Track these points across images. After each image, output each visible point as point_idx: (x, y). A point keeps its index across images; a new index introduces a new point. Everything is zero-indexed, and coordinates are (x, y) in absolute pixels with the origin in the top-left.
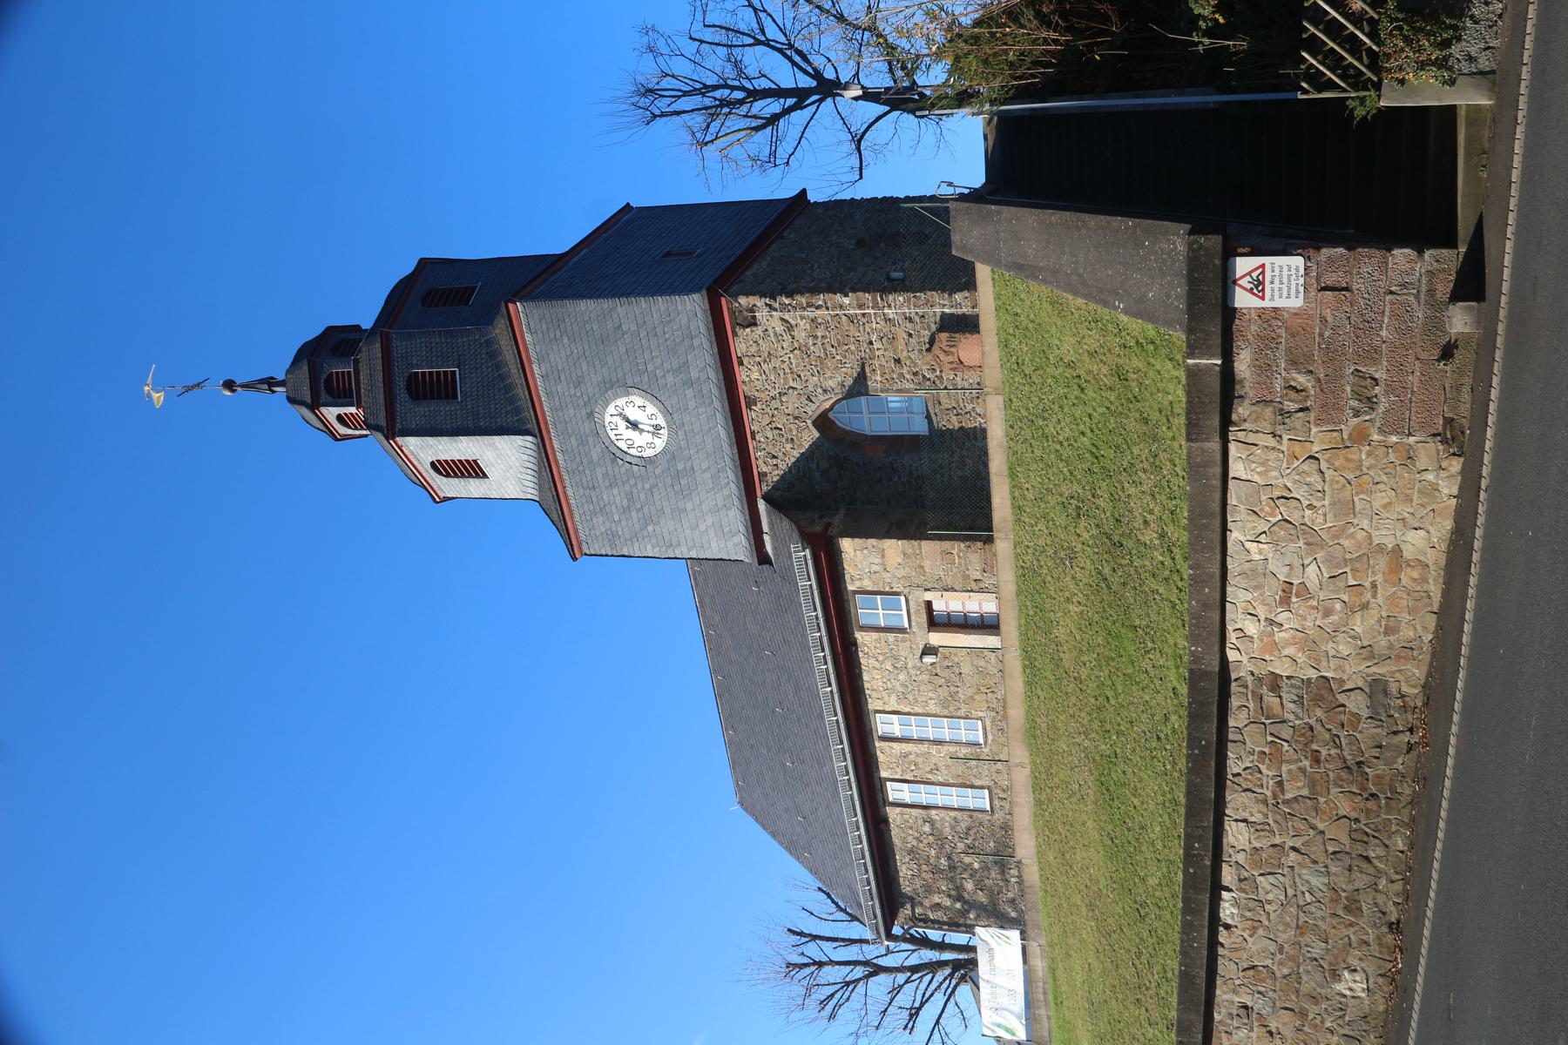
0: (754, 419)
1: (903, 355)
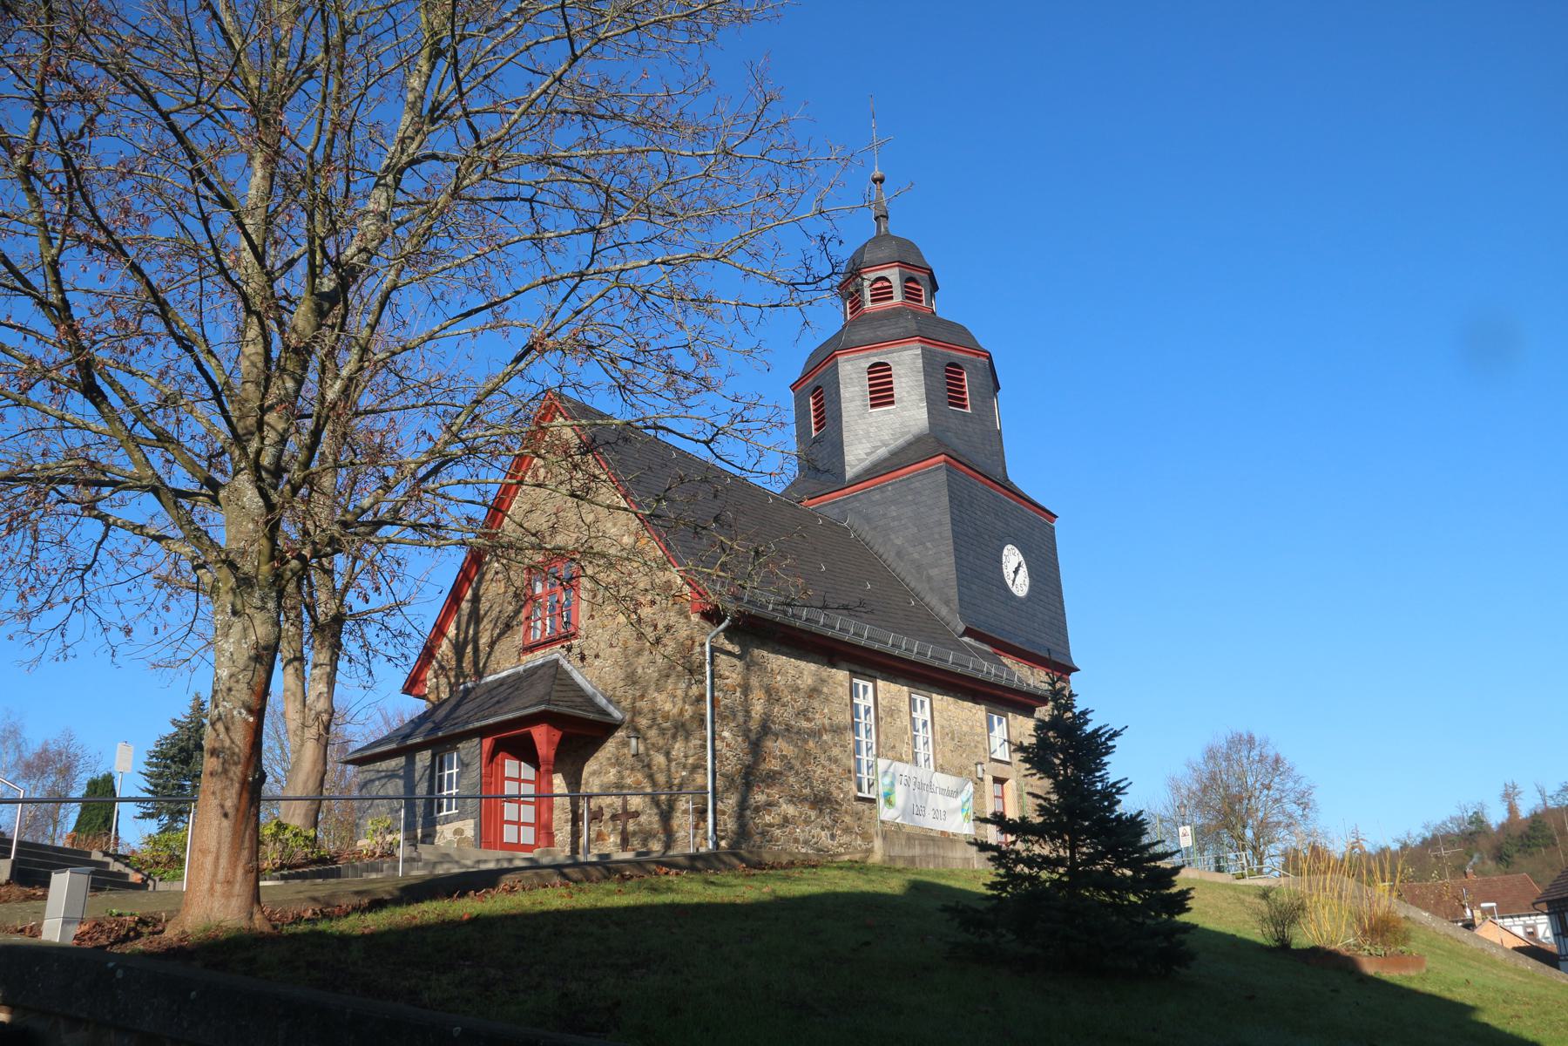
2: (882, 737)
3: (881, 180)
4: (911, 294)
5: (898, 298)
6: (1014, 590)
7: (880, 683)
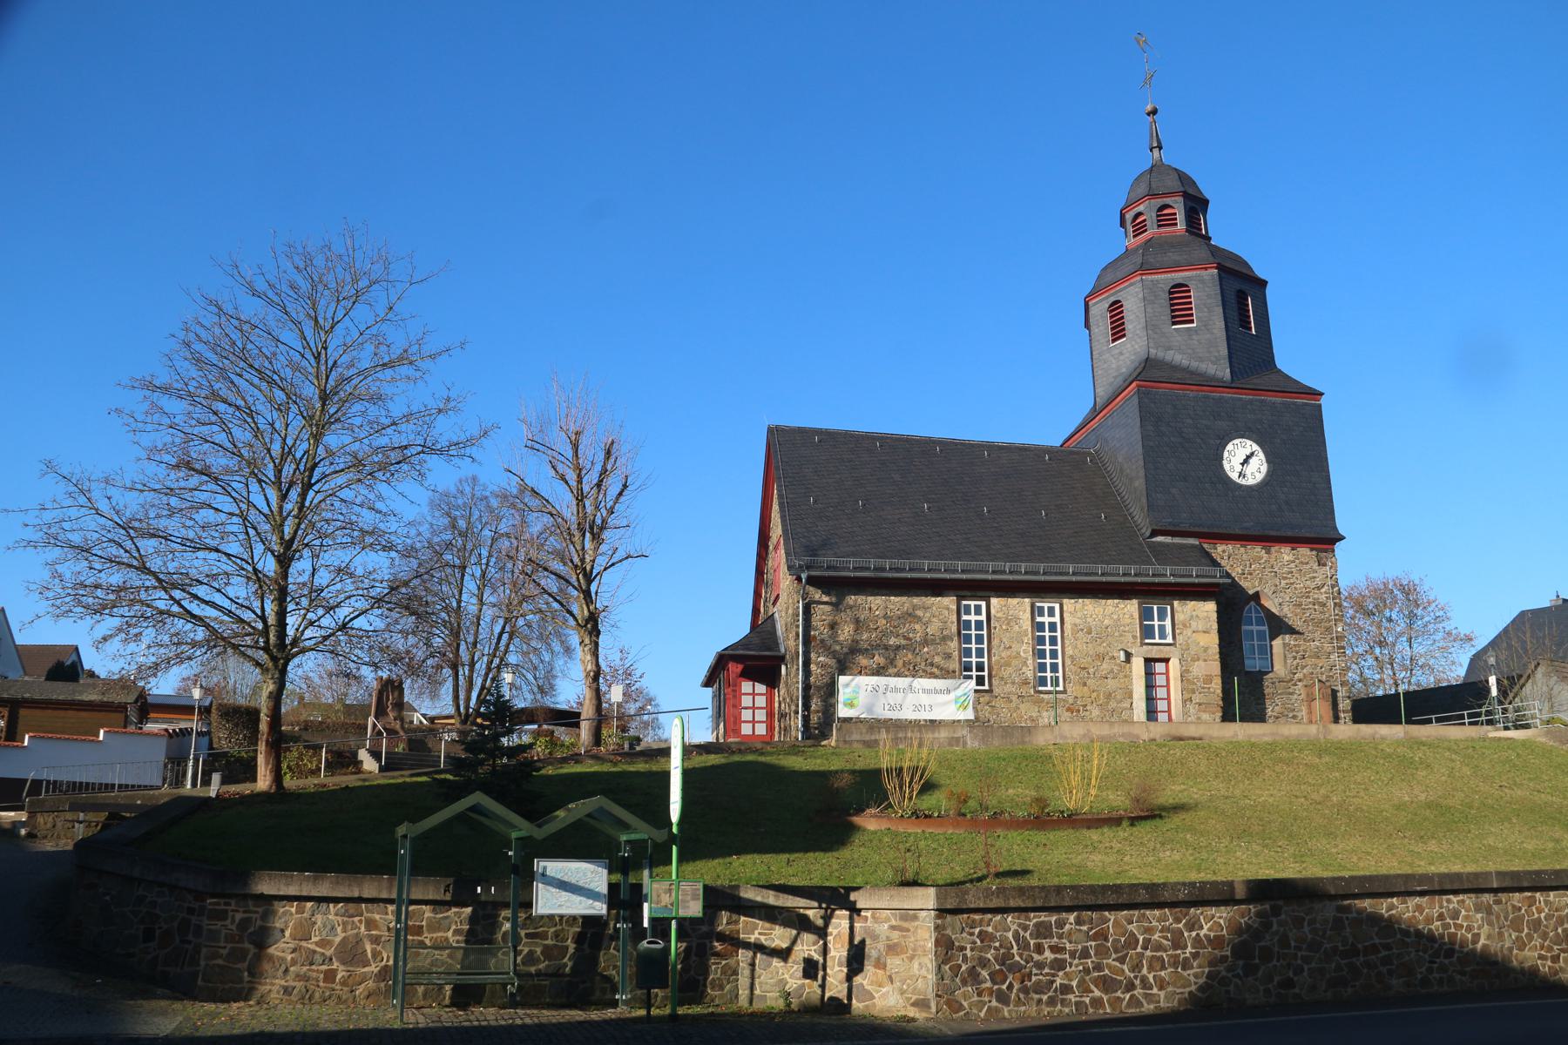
0: (1257, 550)
1: (1309, 661)
2: (995, 642)
3: (1154, 112)
4: (1165, 219)
6: (1243, 482)
7: (994, 601)
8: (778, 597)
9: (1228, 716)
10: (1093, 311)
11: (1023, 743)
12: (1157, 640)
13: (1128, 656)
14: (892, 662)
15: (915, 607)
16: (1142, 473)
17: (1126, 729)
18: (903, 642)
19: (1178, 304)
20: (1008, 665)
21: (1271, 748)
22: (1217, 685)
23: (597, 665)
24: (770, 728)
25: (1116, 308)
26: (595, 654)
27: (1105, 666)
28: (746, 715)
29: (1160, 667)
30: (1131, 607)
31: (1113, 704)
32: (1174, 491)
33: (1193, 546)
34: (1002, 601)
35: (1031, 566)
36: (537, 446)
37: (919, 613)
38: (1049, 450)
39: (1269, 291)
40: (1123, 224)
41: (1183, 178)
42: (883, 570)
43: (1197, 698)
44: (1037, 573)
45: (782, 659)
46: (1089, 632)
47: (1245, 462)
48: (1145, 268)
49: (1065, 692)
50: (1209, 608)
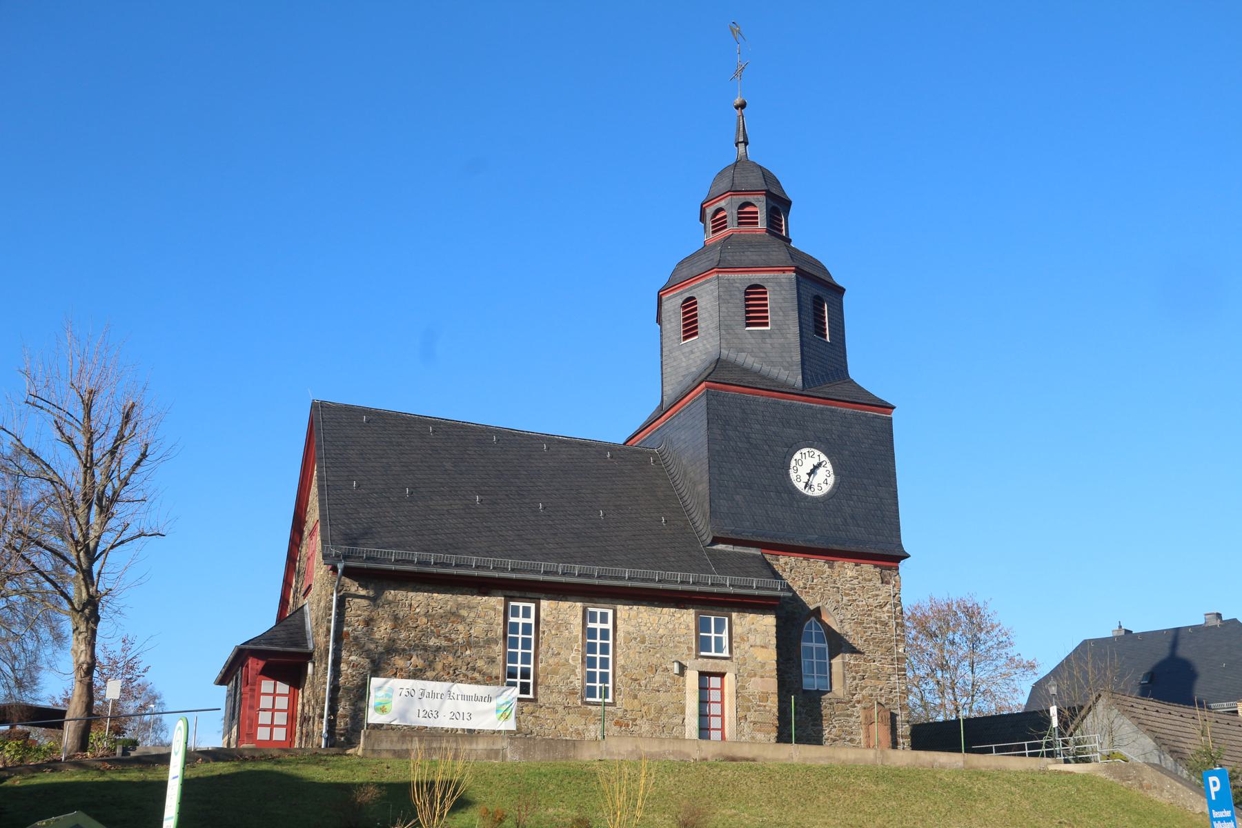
0: (820, 564)
1: (868, 682)
2: (543, 648)
3: (742, 106)
4: (746, 218)
5: (732, 227)
6: (810, 493)
7: (544, 604)
8: (309, 588)
9: (783, 738)
10: (666, 306)
11: (567, 758)
12: (713, 654)
13: (682, 668)
14: (431, 665)
15: (459, 606)
16: (706, 477)
17: (676, 746)
18: (444, 643)
19: (754, 306)
20: (555, 672)
21: (826, 772)
22: (773, 704)
23: (93, 656)
24: (290, 734)
25: (690, 304)
26: (91, 643)
27: (657, 678)
28: (264, 718)
29: (714, 682)
30: (688, 617)
31: (664, 719)
32: (738, 497)
33: (754, 556)
34: (553, 604)
35: (585, 568)
36: (40, 403)
37: (464, 613)
38: (611, 447)
39: (846, 299)
40: (702, 218)
41: (767, 176)
42: (427, 564)
43: (752, 716)
44: (591, 576)
45: (309, 656)
46: (643, 642)
47: (812, 473)
48: (722, 266)
49: (614, 704)
50: (768, 622)
